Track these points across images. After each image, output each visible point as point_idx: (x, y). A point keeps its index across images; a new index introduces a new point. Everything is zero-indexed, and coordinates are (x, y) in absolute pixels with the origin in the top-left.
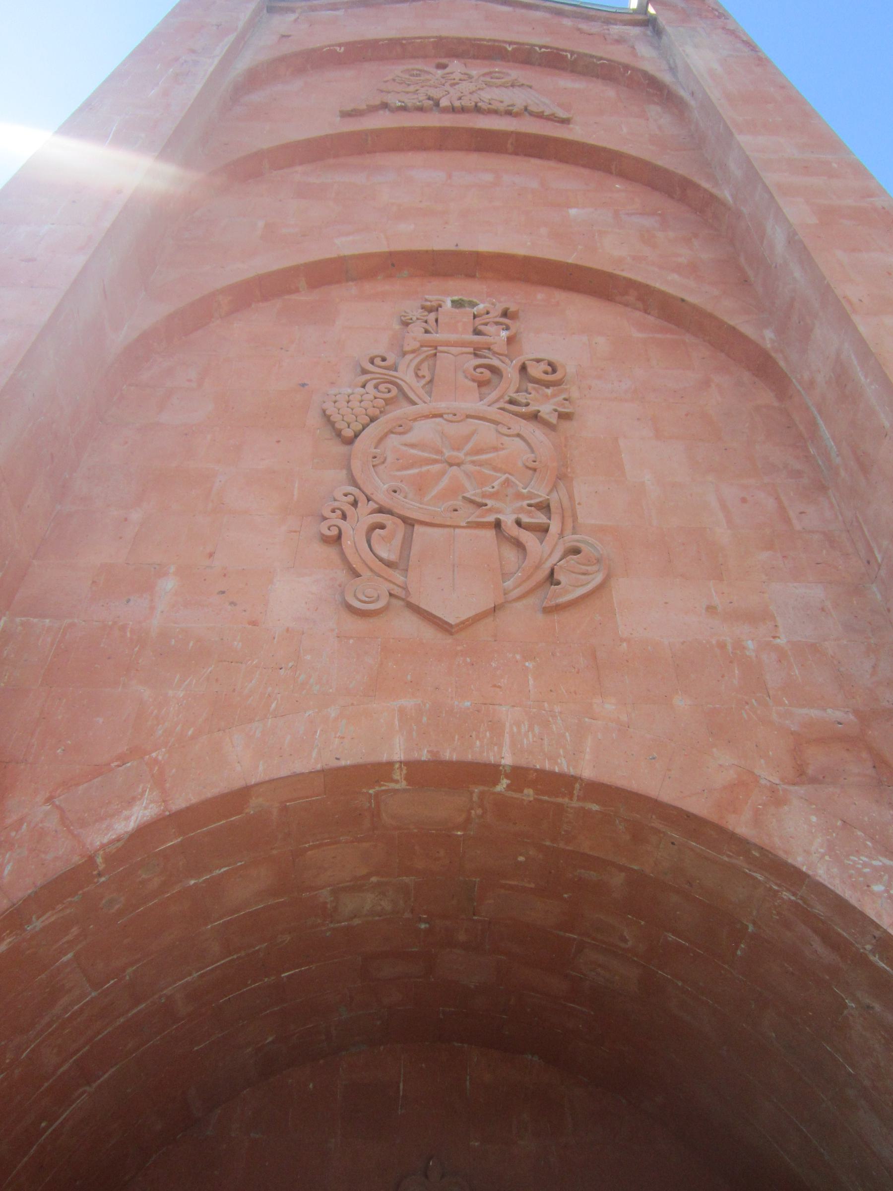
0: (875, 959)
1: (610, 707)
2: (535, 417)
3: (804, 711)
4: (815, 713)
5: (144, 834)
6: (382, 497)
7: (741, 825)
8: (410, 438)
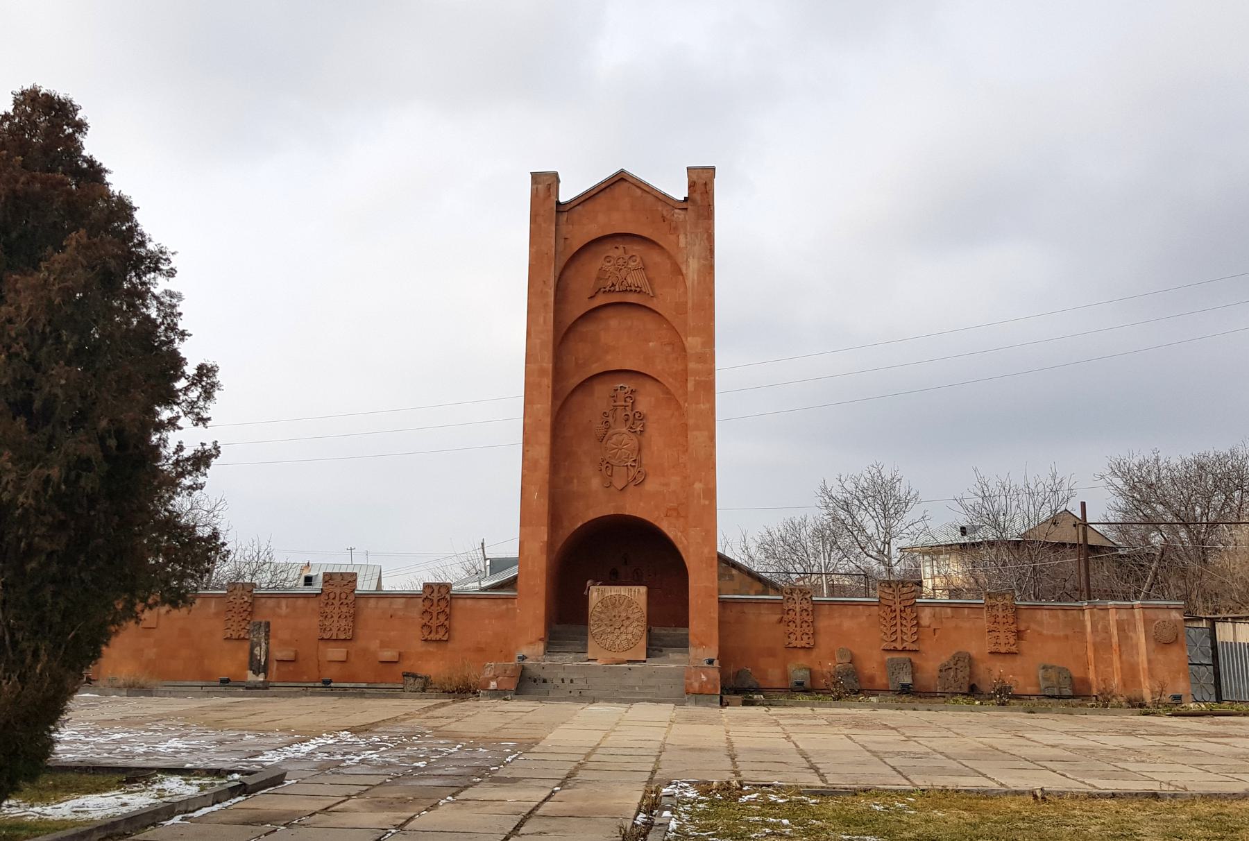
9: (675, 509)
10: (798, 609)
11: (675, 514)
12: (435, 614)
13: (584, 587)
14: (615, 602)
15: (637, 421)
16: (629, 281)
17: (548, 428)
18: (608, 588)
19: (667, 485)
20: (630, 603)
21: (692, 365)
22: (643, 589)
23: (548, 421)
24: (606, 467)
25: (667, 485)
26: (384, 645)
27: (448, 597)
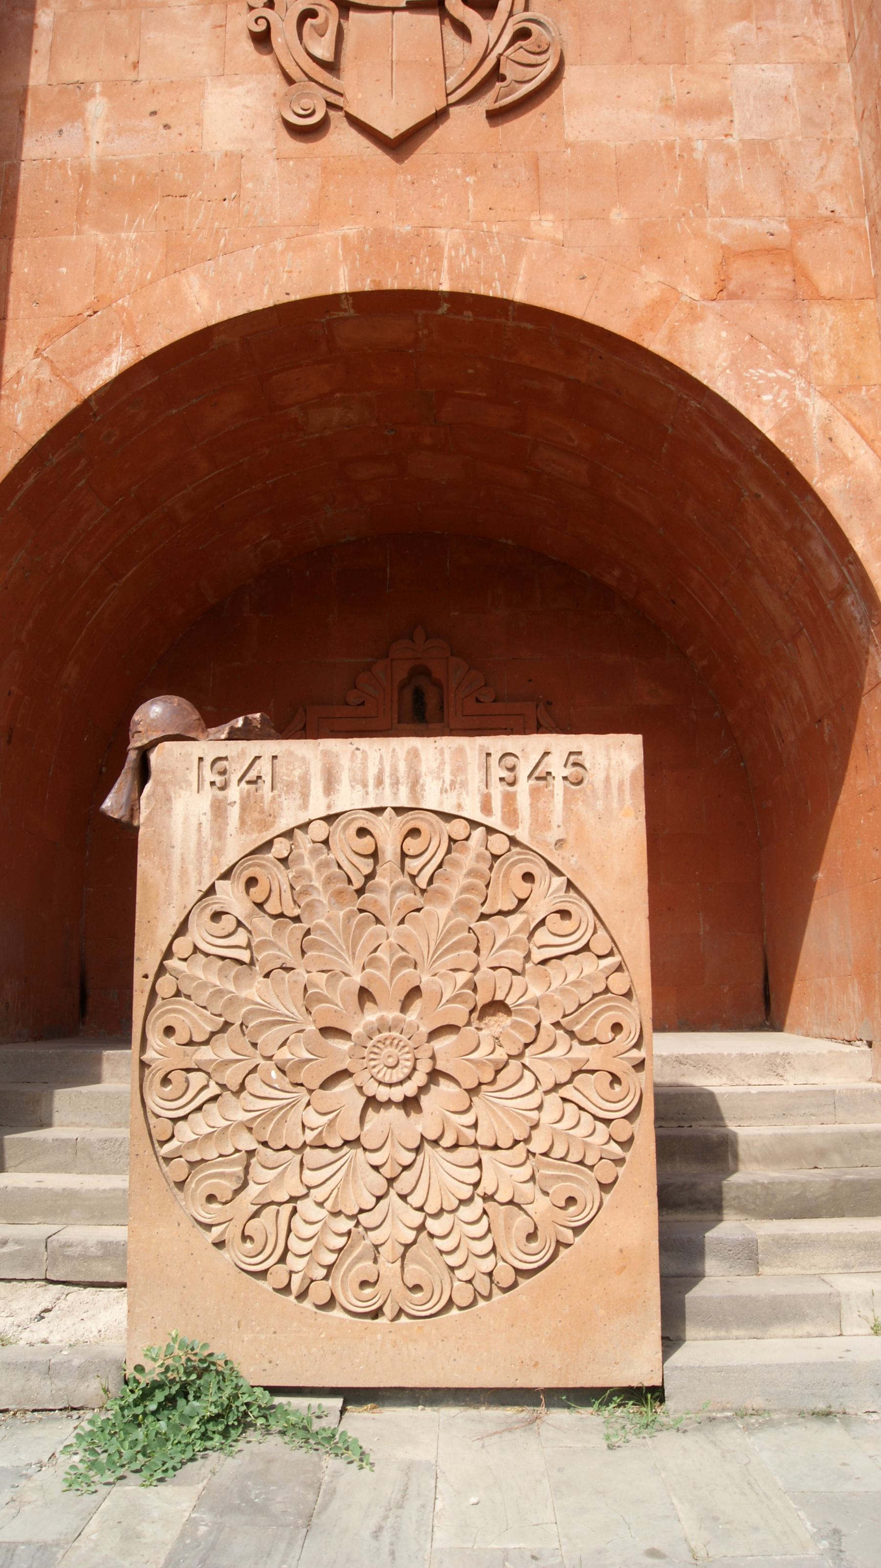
0: (759, 457)
1: (546, 225)
3: (739, 222)
4: (748, 224)
7: (656, 345)
9: (776, 253)
11: (777, 282)
13: (110, 753)
14: (380, 865)
18: (306, 754)
19: (715, 109)
22: (617, 758)
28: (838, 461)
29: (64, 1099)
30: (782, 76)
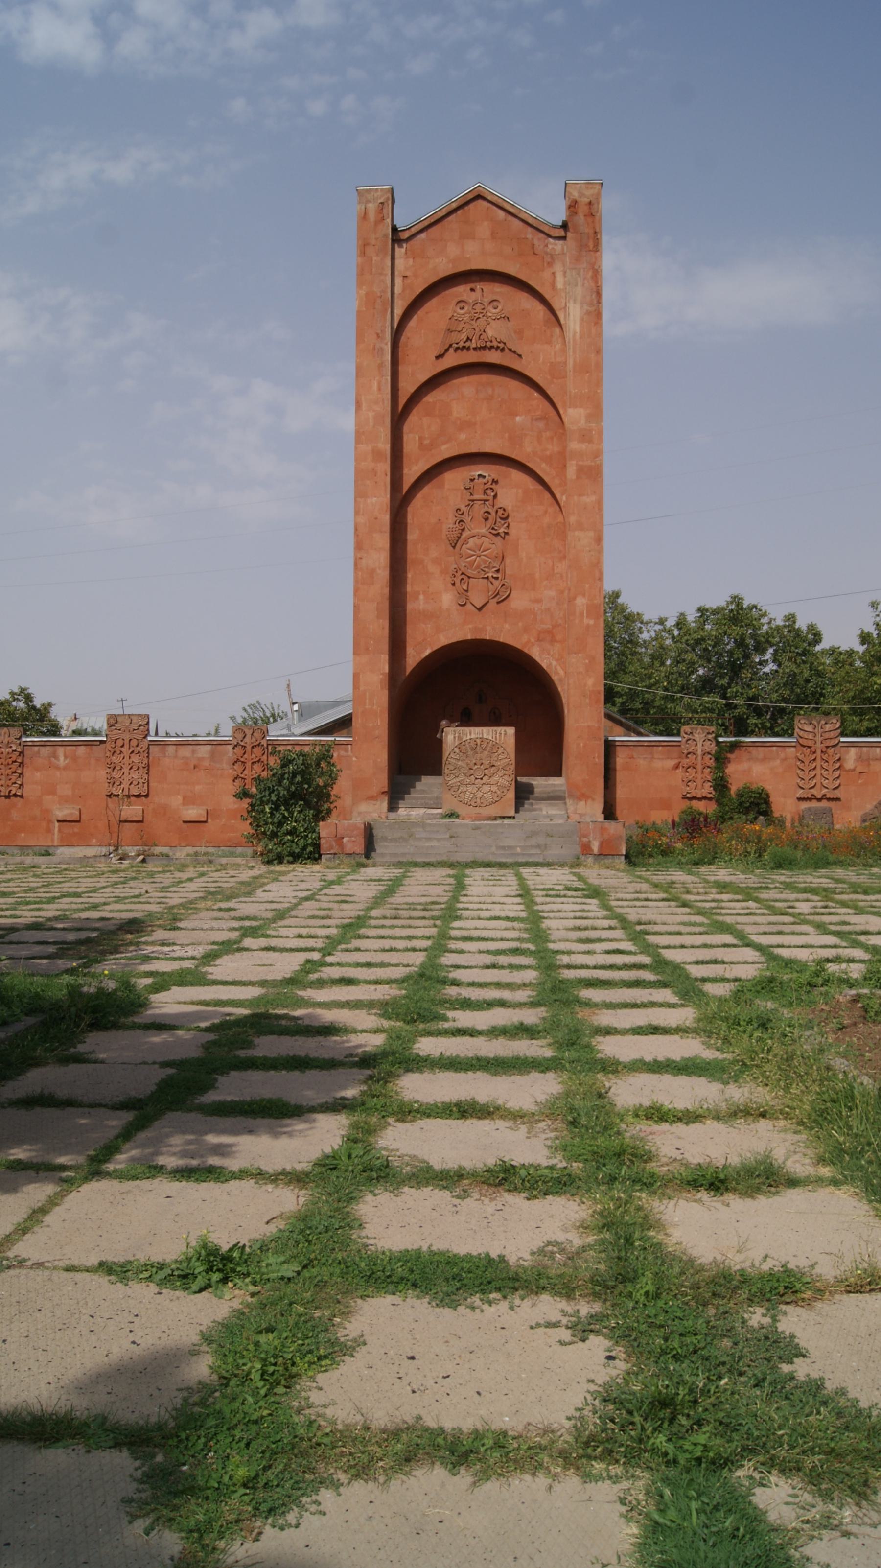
1: (507, 626)
2: (498, 534)
5: (430, 655)
6: (463, 569)
7: (526, 651)
8: (469, 546)
9: (549, 632)
10: (699, 752)
12: (249, 764)
13: (437, 728)
14: (477, 746)
15: (499, 522)
16: (490, 333)
17: (387, 528)
18: (467, 729)
19: (538, 601)
20: (495, 747)
21: (574, 445)
22: (511, 731)
23: (386, 518)
24: (460, 579)
25: (538, 601)
26: (189, 800)
27: (264, 742)
28: (557, 673)
29: (417, 784)
30: (552, 593)
